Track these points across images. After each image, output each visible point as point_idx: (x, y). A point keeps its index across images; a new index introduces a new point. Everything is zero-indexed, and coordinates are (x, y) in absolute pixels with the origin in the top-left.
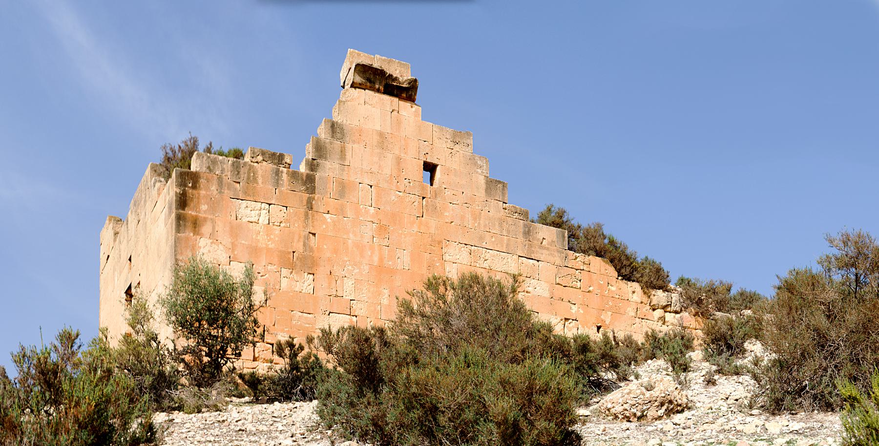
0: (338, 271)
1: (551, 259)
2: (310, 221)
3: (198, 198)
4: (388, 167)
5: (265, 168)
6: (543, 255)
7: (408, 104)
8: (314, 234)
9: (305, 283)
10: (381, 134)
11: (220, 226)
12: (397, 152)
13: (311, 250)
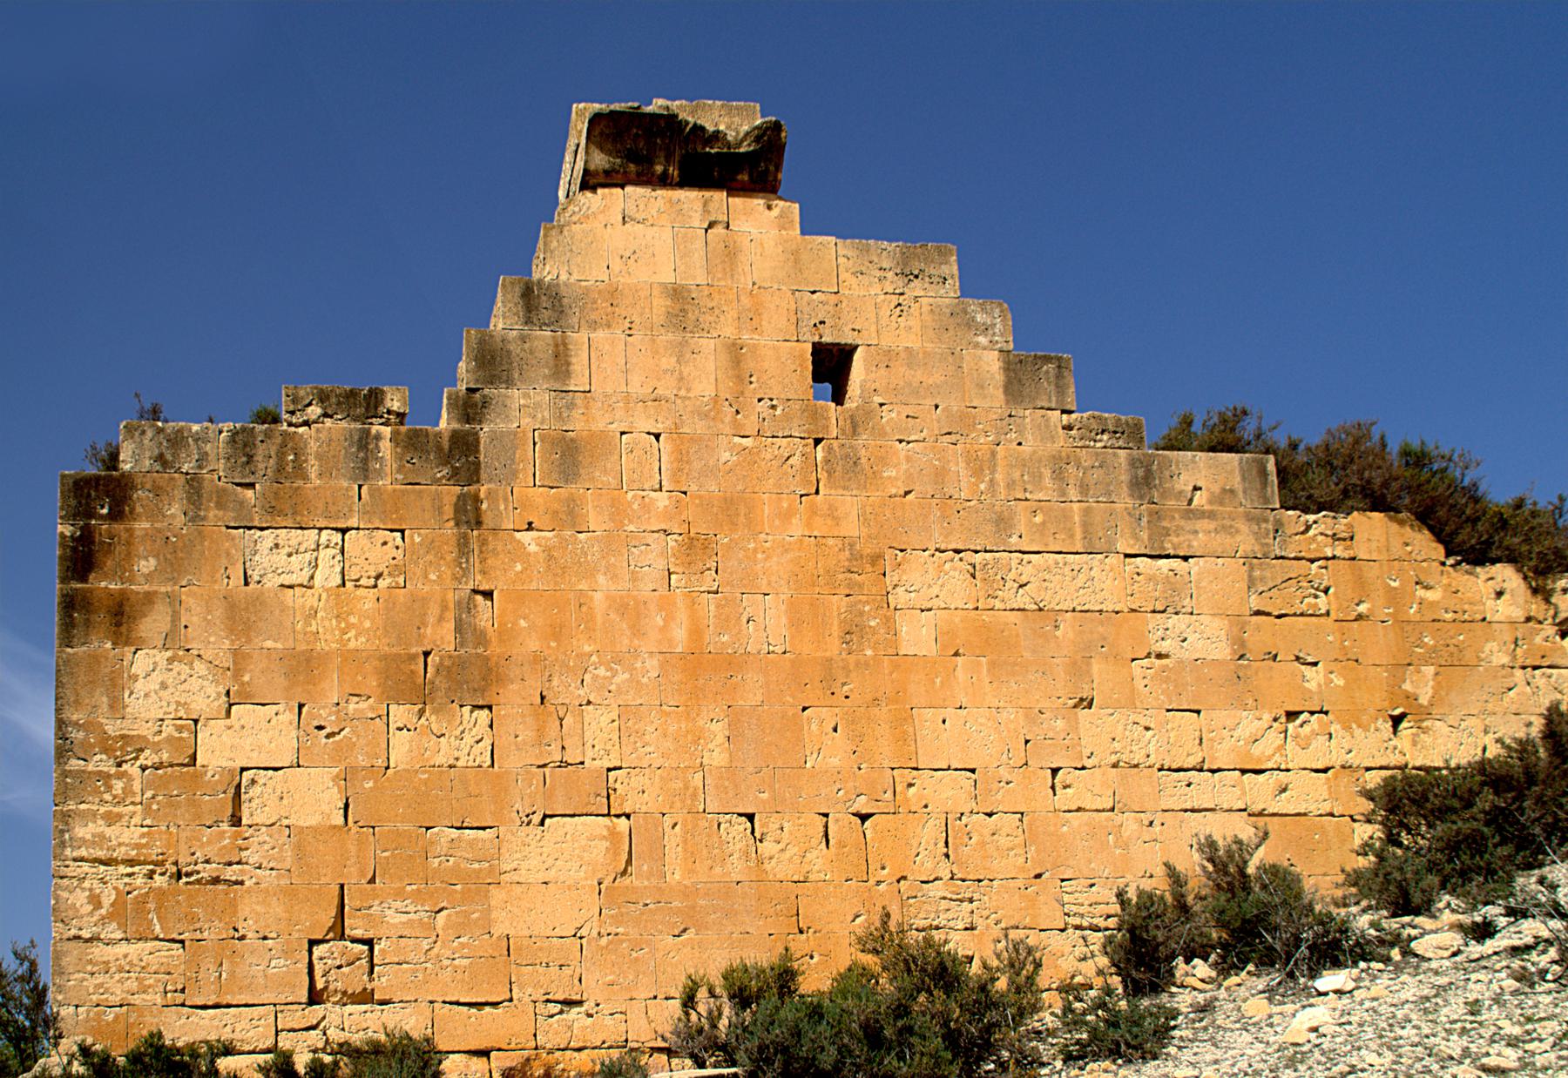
0: (564, 690)
1: (1221, 542)
2: (475, 558)
3: (129, 543)
4: (706, 376)
5: (323, 435)
6: (1201, 537)
7: (758, 203)
8: (488, 595)
9: (462, 738)
10: (677, 293)
11: (193, 616)
12: (729, 331)
13: (481, 638)
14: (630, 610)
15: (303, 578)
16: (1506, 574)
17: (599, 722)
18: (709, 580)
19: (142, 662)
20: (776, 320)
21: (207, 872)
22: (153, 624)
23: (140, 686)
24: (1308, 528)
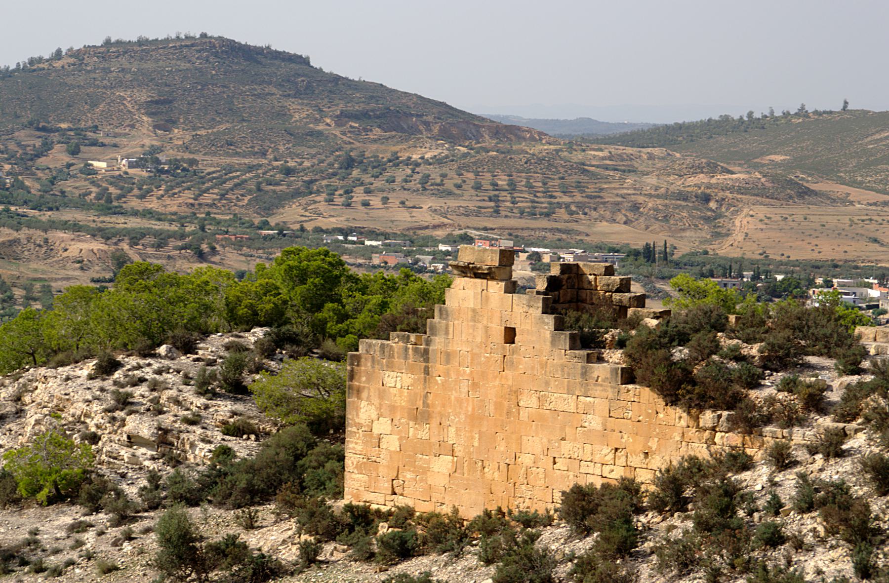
1: (604, 394)
6: (598, 391)
9: (423, 433)
10: (474, 310)
12: (485, 322)
13: (428, 406)
14: (459, 401)
15: (393, 385)
17: (452, 430)
19: (363, 404)
20: (496, 320)
21: (374, 459)
22: (364, 395)
23: (362, 410)
24: (628, 391)
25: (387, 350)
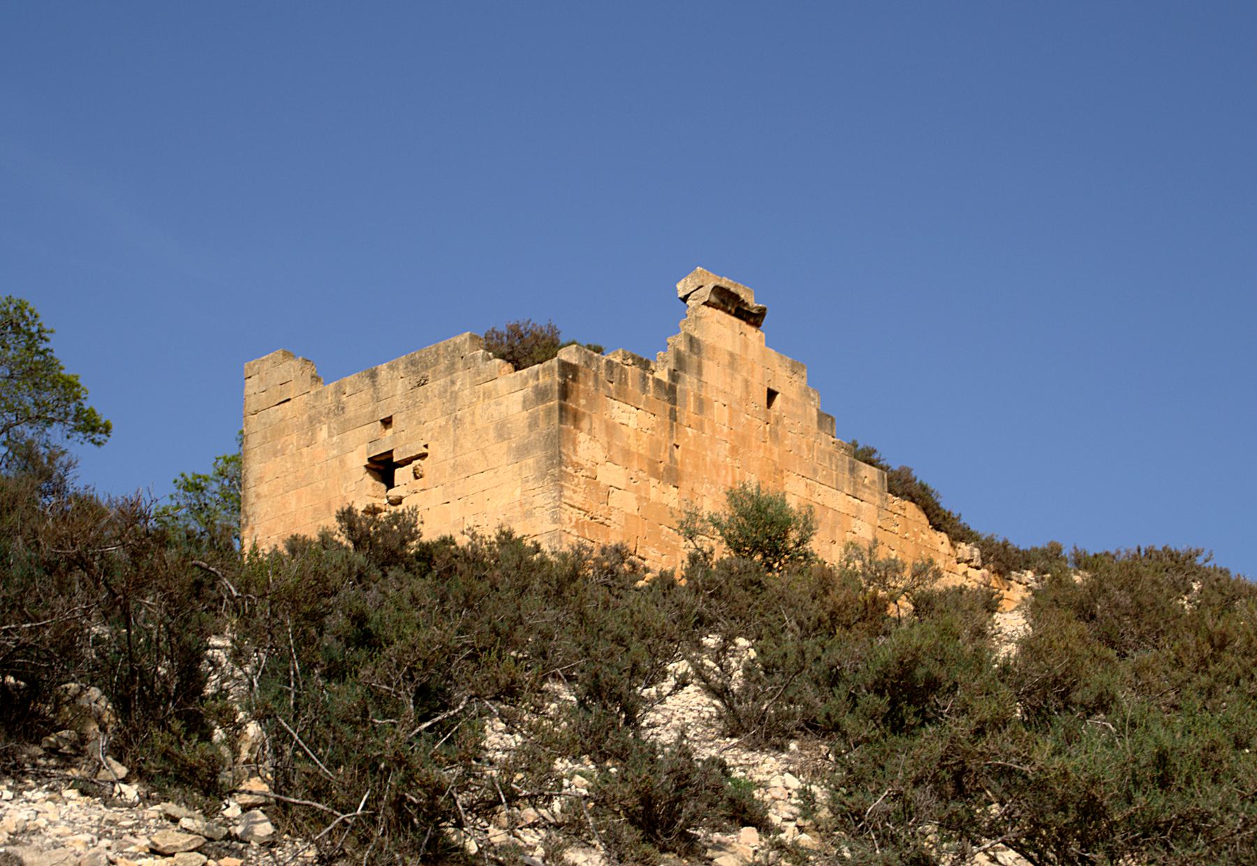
1: (871, 498)
7: (754, 329)
10: (731, 355)
13: (676, 463)
16: (944, 536)
18: (737, 464)
21: (601, 519)
22: (585, 424)
25: (616, 371)
